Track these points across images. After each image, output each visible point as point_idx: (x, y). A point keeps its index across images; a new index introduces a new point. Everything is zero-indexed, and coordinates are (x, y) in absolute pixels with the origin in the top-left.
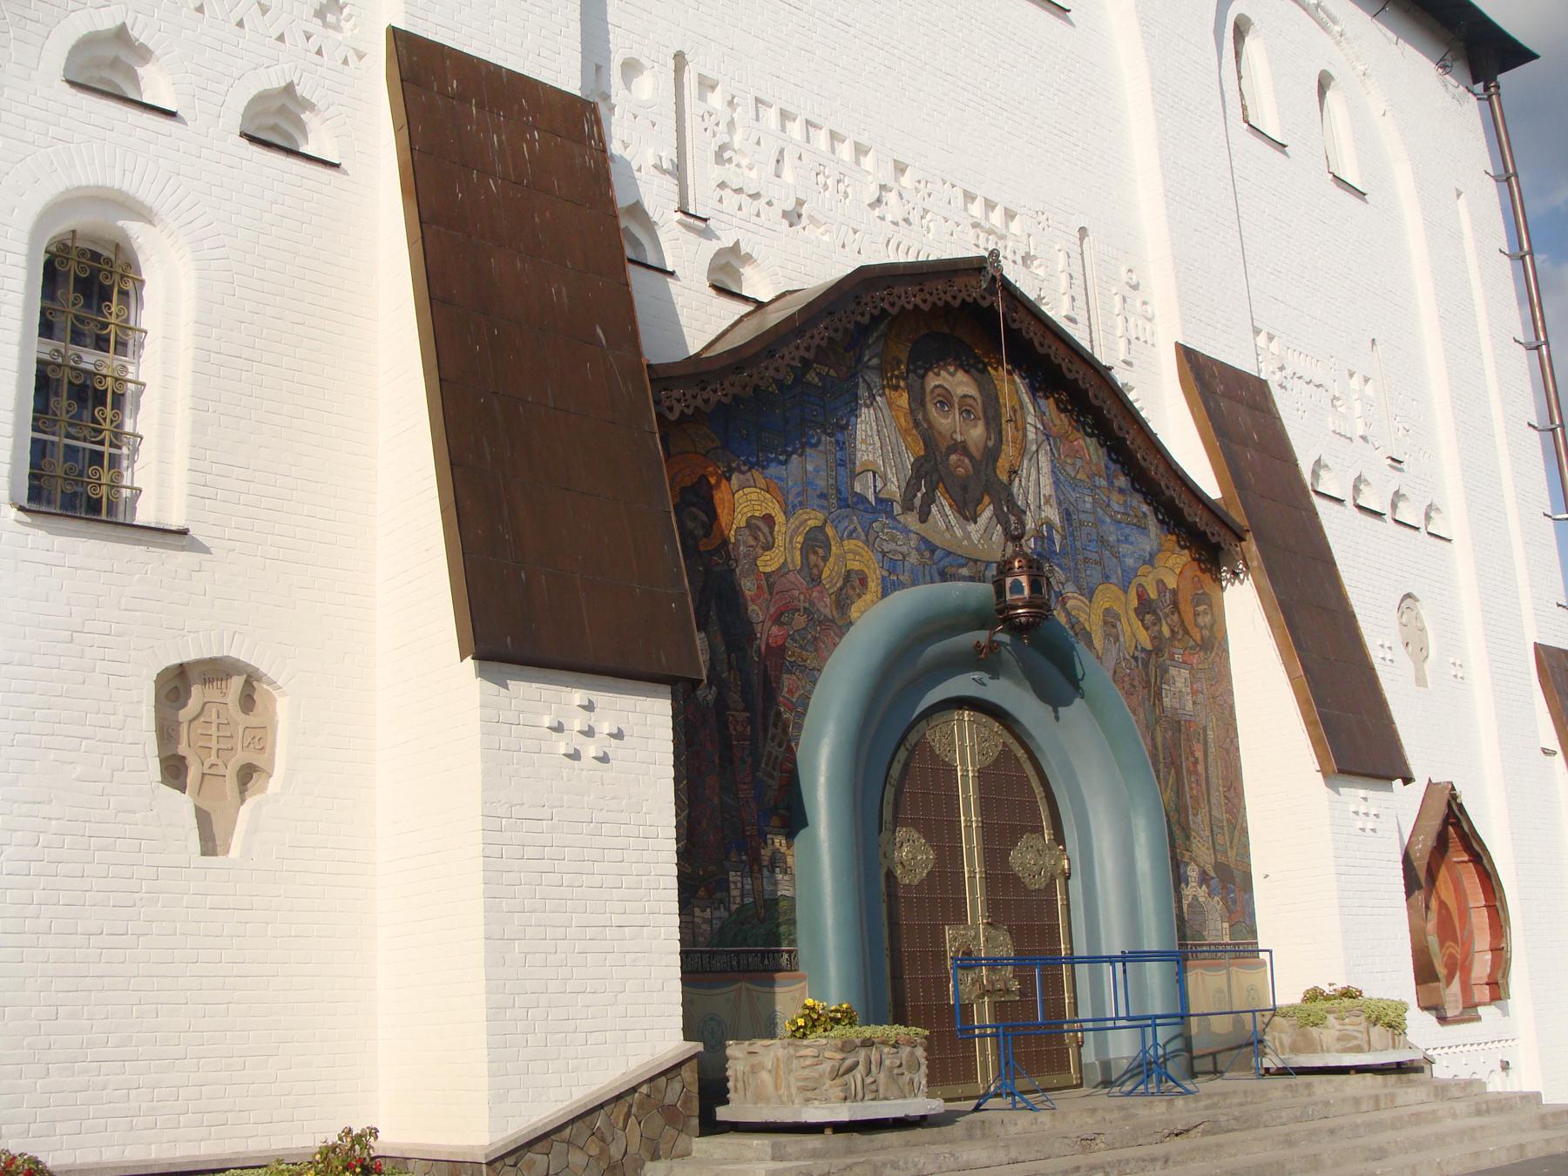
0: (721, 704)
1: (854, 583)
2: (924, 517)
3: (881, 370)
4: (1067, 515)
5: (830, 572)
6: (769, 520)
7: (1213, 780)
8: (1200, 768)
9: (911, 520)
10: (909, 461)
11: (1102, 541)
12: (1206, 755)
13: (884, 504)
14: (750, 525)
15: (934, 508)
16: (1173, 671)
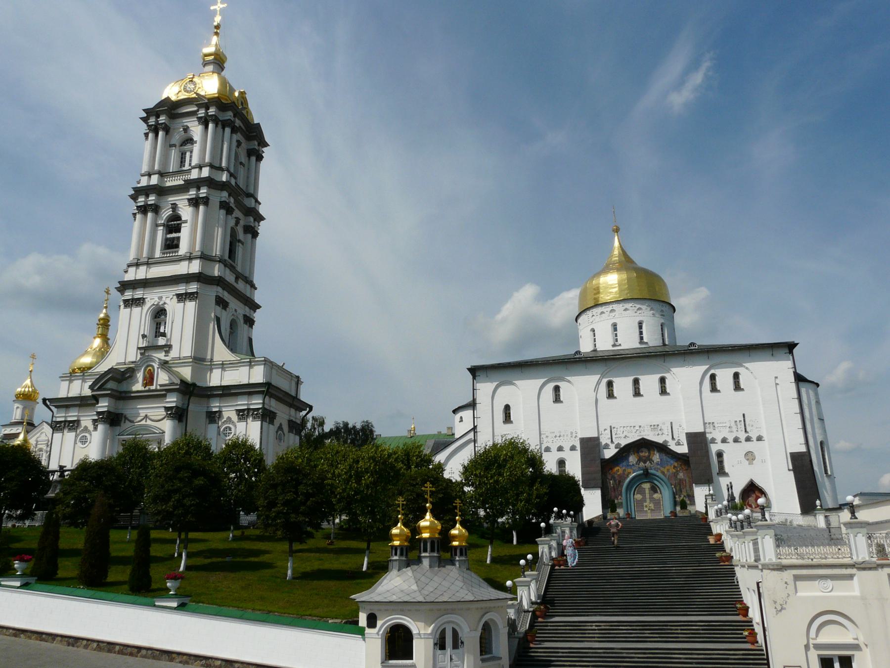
0: (614, 486)
1: (629, 473)
2: (639, 465)
3: (633, 452)
4: (661, 460)
5: (626, 473)
6: (619, 470)
7: (687, 484)
8: (685, 484)
9: (637, 465)
10: (637, 460)
11: (667, 461)
12: (686, 483)
13: (633, 465)
14: (617, 471)
15: (640, 464)
16: (680, 474)
